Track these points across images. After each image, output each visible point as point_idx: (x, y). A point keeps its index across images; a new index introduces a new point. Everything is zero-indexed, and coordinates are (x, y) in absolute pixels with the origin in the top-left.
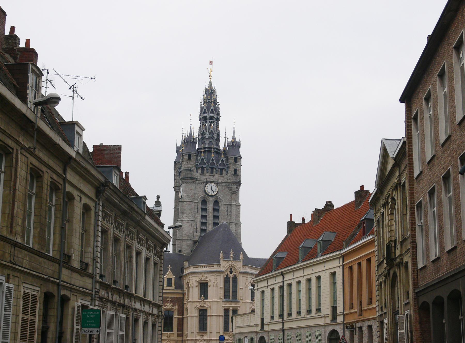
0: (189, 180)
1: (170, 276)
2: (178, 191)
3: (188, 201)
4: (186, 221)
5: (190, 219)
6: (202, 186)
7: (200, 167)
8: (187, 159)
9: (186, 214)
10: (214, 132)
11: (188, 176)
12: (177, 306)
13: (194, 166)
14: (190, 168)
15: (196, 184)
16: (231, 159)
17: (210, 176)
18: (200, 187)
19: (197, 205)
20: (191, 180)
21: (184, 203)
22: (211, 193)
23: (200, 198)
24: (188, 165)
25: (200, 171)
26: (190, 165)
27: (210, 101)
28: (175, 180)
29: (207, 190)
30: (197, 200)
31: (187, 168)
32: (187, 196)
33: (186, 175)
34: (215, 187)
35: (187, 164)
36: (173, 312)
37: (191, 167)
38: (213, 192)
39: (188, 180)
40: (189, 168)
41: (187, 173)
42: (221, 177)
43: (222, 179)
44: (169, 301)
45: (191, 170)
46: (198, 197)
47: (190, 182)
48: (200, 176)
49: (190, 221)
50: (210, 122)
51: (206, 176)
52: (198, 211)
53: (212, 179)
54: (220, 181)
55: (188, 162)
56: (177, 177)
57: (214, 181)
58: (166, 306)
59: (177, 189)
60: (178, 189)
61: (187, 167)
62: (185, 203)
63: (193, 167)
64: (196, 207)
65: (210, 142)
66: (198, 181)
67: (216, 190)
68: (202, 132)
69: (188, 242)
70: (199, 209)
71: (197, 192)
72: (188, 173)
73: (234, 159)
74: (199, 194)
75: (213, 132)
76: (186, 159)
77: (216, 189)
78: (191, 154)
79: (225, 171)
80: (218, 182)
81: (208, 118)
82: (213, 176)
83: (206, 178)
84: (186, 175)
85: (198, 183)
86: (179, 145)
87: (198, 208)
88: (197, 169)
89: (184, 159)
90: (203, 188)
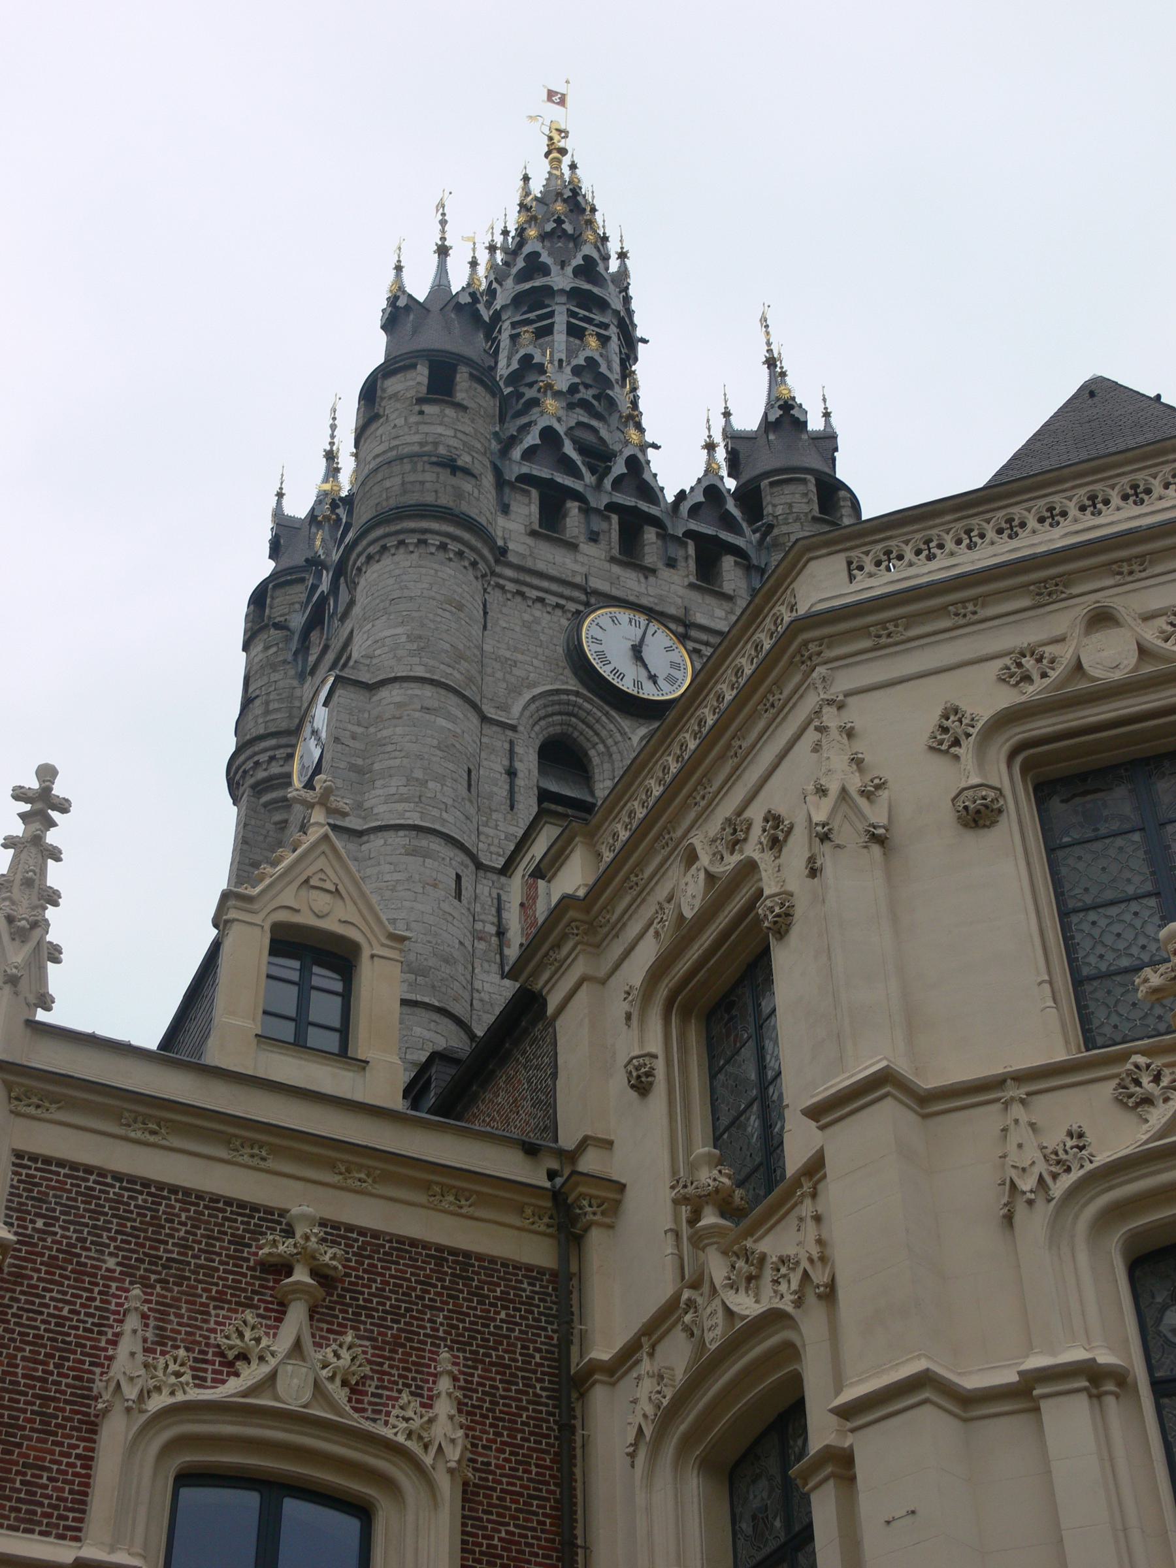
0: (435, 526)
1: (322, 901)
2: (275, 769)
3: (428, 675)
4: (399, 840)
5: (437, 827)
6: (552, 625)
7: (526, 479)
8: (424, 389)
9: (395, 782)
10: (610, 368)
11: (430, 498)
12: (444, 1408)
13: (479, 446)
14: (442, 450)
15: (495, 597)
16: (788, 489)
17: (616, 569)
18: (525, 624)
19: (501, 745)
20: (451, 529)
21: (384, 693)
22: (638, 684)
23: (527, 696)
24: (424, 428)
25: (527, 510)
26: (451, 433)
27: (568, 227)
28: (257, 708)
29: (601, 655)
30: (504, 708)
31: (416, 448)
32: (411, 638)
33: (405, 492)
34: (668, 649)
35: (414, 419)
36: (363, 1512)
37: (453, 442)
38: (653, 678)
39: (424, 524)
40: (436, 444)
41: (411, 478)
42: (710, 600)
43: (720, 613)
44: (301, 1275)
45: (455, 460)
46: (515, 690)
47: (443, 547)
48: (530, 541)
49: (436, 845)
50: (572, 314)
51: (580, 558)
52: (512, 792)
53: (630, 583)
54: (701, 619)
55: (427, 409)
56: (275, 676)
57: (658, 608)
58: (231, 1364)
59: (263, 758)
60: (280, 753)
61: (417, 438)
62: (391, 695)
63: (469, 448)
64: (495, 766)
65: (580, 424)
66: (509, 573)
67: (678, 674)
68: (515, 365)
69: (418, 1030)
70: (520, 782)
71: (508, 654)
72: (429, 477)
73: (812, 487)
74: (516, 671)
75: (603, 369)
76: (412, 393)
77: (674, 665)
78: (453, 369)
79: (739, 572)
80: (688, 625)
81: (562, 291)
82: (649, 572)
83: (584, 570)
84: (405, 492)
85: (510, 586)
86: (299, 507)
87: (511, 773)
88: (501, 482)
89: (395, 396)
90: (561, 639)
